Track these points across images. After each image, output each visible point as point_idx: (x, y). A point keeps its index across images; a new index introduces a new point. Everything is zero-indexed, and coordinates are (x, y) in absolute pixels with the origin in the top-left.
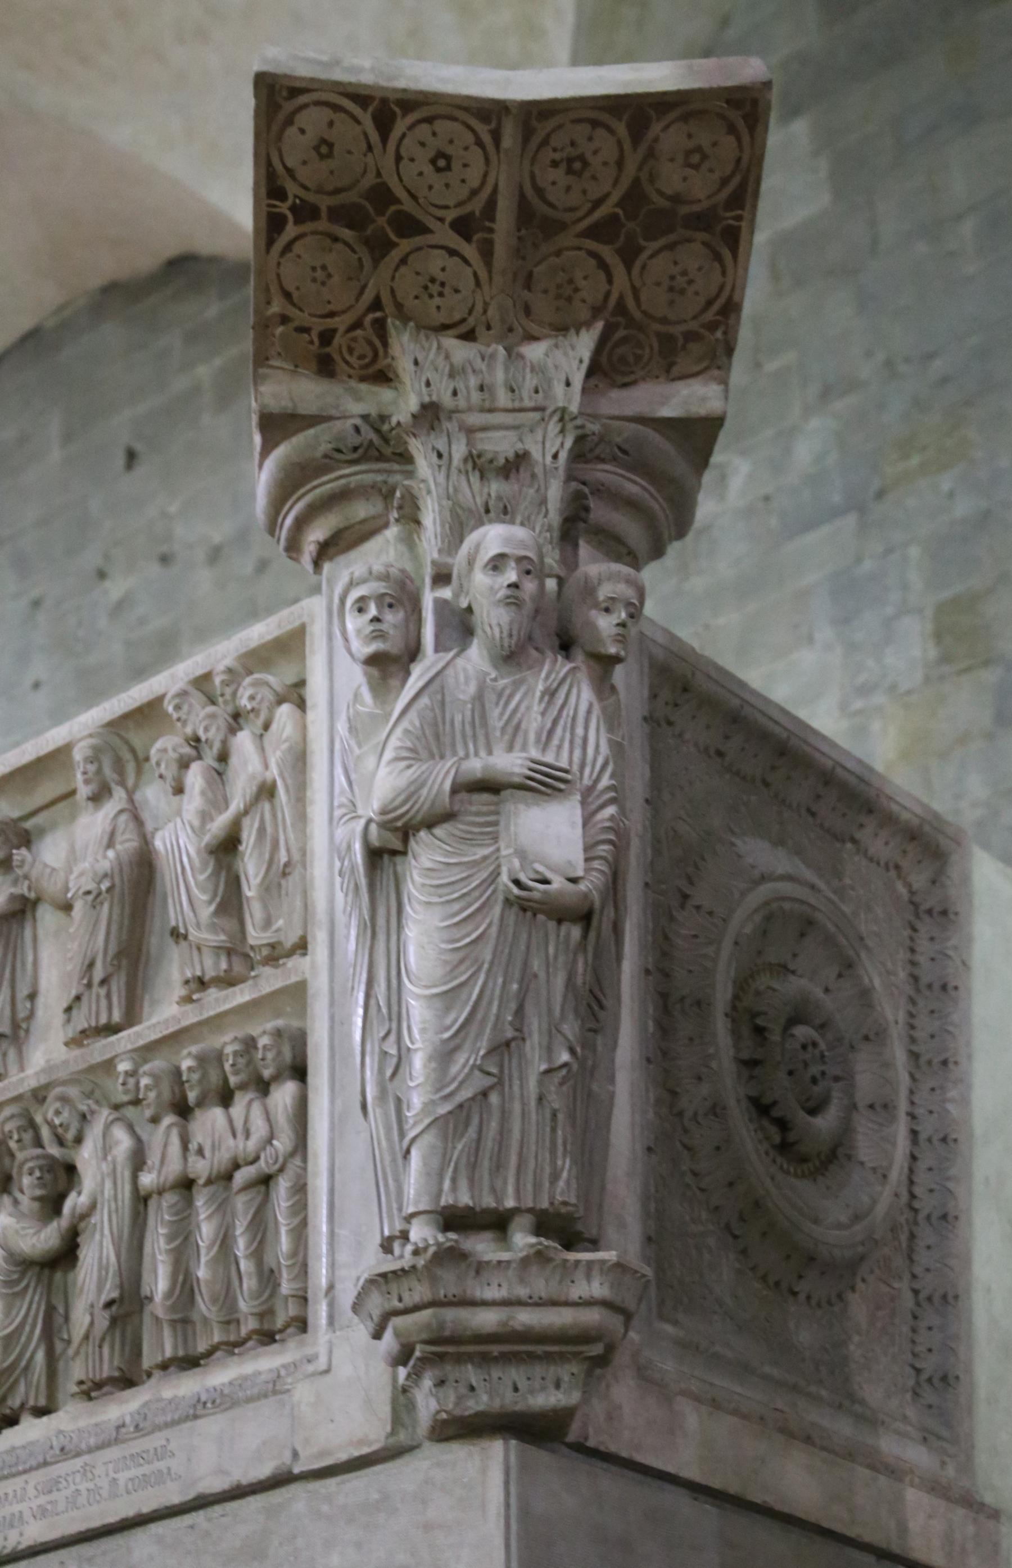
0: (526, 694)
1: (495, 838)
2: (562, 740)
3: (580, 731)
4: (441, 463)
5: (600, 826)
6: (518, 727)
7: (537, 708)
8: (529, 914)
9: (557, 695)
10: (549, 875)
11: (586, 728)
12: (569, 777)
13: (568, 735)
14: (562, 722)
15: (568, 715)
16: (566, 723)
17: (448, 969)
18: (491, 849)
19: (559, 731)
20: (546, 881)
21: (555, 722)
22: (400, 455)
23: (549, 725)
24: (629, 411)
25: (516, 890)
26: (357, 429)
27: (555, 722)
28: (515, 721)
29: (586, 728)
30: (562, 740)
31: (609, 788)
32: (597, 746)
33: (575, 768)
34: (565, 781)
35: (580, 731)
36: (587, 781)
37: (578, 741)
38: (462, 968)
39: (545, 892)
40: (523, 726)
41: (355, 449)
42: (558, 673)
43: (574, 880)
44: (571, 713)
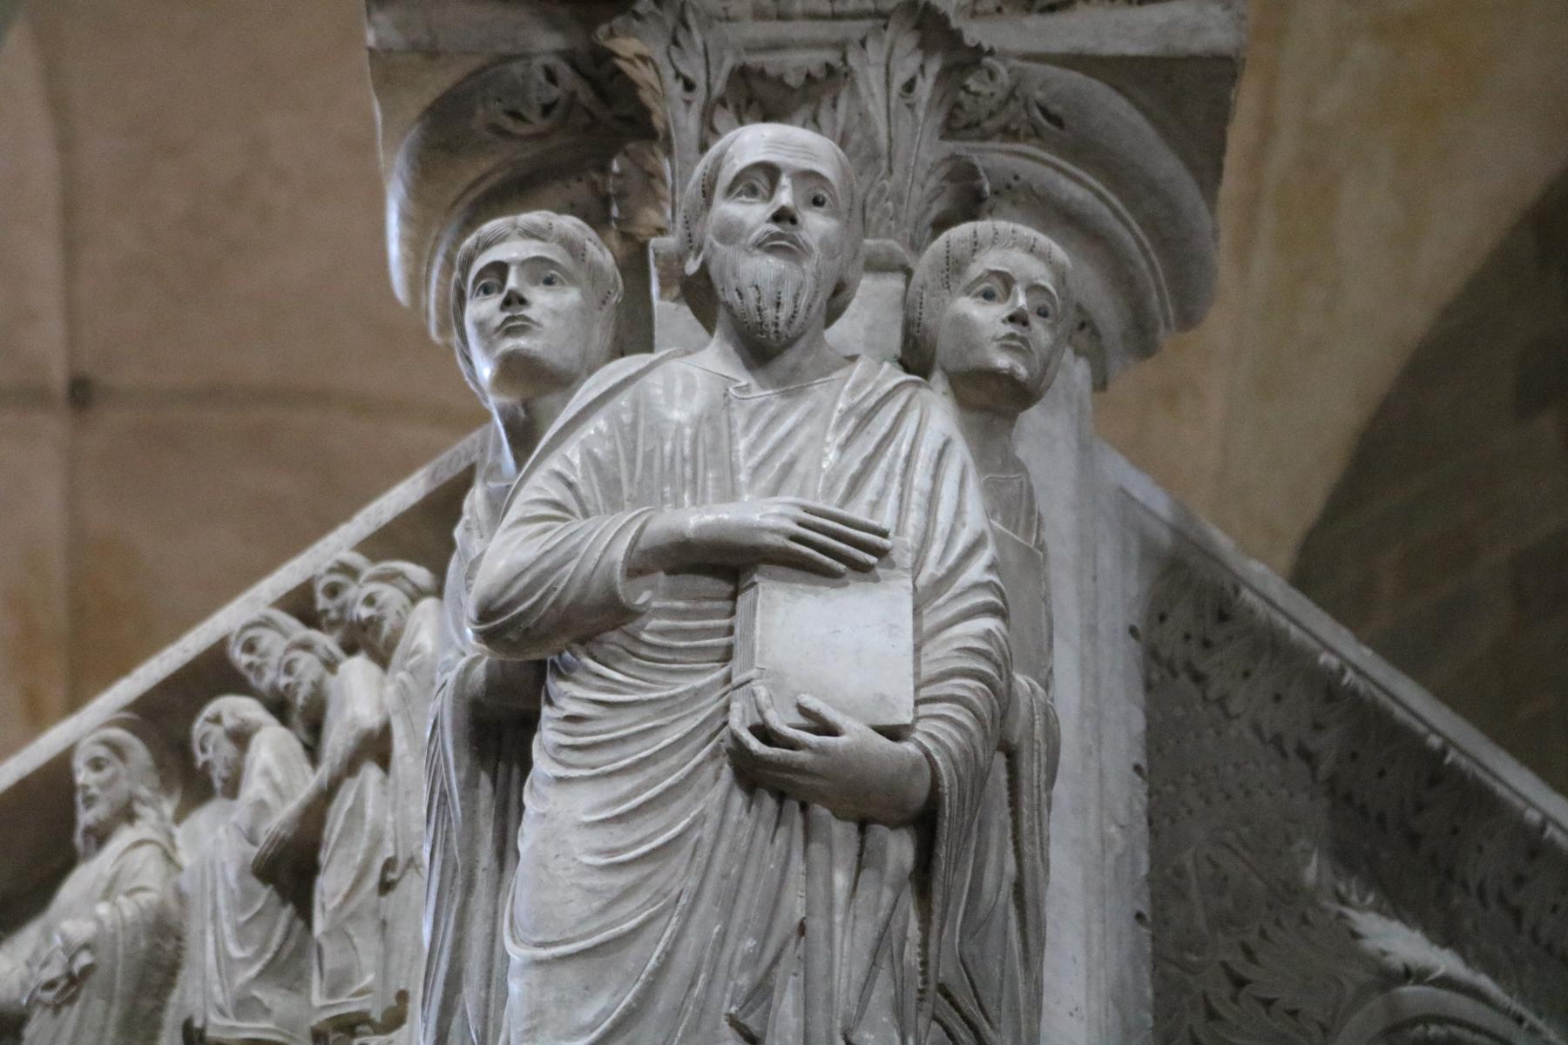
0: (811, 414)
1: (727, 655)
2: (882, 493)
3: (921, 478)
4: (688, 96)
5: (956, 645)
6: (789, 467)
7: (834, 439)
8: (793, 806)
9: (876, 420)
10: (833, 716)
11: (936, 477)
12: (887, 543)
13: (895, 488)
14: (883, 464)
15: (896, 455)
16: (891, 466)
17: (596, 904)
18: (720, 673)
19: (876, 479)
20: (830, 730)
21: (869, 463)
22: (629, 120)
23: (855, 466)
24: (1058, 46)
25: (755, 745)
26: (551, 76)
27: (869, 463)
28: (785, 457)
29: (936, 477)
30: (882, 493)
31: (977, 586)
32: (959, 512)
33: (910, 538)
34: (881, 552)
35: (921, 478)
36: (931, 570)
37: (916, 499)
38: (631, 905)
39: (821, 750)
40: (800, 468)
41: (547, 109)
42: (879, 384)
43: (894, 733)
44: (905, 449)
